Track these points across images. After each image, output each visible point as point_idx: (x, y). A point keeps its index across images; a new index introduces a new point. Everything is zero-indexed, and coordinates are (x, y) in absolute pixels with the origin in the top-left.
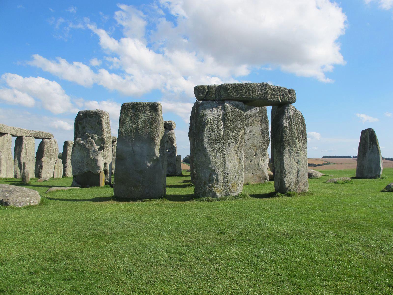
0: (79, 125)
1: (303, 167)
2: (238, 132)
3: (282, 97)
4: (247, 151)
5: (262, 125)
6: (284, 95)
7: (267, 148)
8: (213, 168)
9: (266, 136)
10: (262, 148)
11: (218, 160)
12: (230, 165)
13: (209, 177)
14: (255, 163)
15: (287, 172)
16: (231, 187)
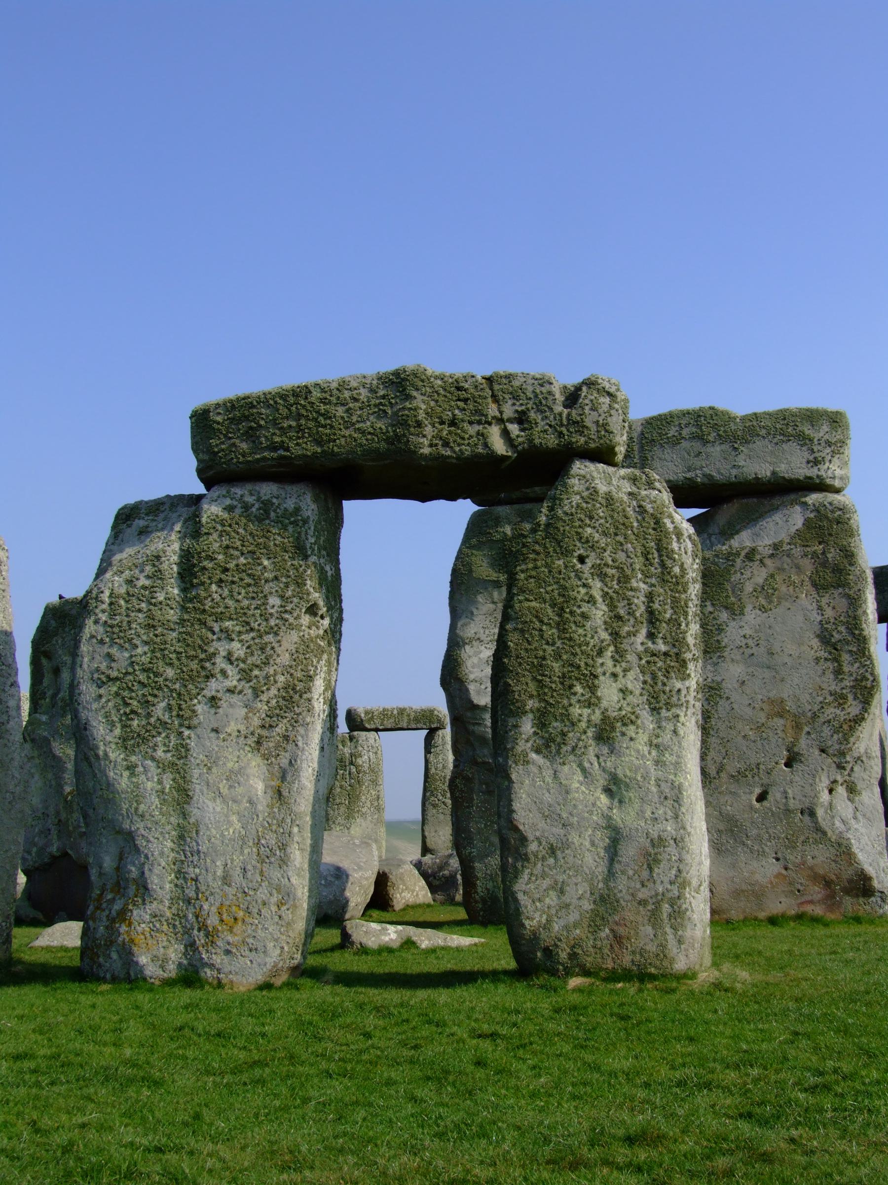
0: (44, 661)
1: (648, 814)
2: (270, 638)
3: (514, 428)
4: (740, 738)
5: (824, 601)
6: (532, 415)
7: (859, 720)
8: (126, 825)
9: (846, 657)
10: (829, 721)
11: (149, 785)
12: (218, 809)
13: (118, 869)
14: (786, 804)
15: (533, 847)
16: (213, 921)
